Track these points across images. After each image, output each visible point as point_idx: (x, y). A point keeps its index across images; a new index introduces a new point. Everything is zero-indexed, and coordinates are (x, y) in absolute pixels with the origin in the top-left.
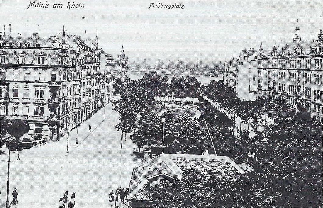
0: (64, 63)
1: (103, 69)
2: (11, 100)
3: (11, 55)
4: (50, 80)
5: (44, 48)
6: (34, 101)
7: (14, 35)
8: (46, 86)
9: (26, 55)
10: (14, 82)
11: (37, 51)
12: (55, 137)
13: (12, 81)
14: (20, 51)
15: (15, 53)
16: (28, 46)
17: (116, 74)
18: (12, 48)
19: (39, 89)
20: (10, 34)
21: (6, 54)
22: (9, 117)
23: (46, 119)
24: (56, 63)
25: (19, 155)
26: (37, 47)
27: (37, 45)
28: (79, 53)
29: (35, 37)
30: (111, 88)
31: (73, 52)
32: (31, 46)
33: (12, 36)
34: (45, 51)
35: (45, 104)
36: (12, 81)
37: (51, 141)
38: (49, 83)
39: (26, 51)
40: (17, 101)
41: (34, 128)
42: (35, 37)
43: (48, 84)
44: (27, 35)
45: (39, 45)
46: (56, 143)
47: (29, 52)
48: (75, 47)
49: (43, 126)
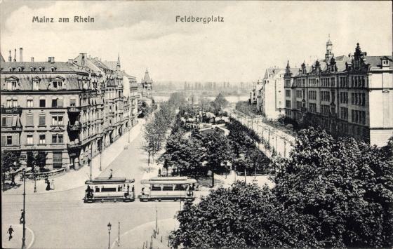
0: (350, 78)
1: (126, 93)
2: (24, 129)
3: (24, 81)
4: (69, 106)
5: (62, 72)
6: (51, 129)
7: (27, 59)
8: (64, 112)
9: (40, 80)
10: (27, 109)
11: (53, 75)
12: (76, 165)
13: (24, 109)
14: (34, 75)
15: (28, 78)
16: (43, 71)
17: (141, 97)
18: (56, 73)
19: (58, 115)
20: (21, 58)
21: (18, 80)
22: (23, 148)
23: (65, 147)
24: (74, 88)
25: (137, 201)
26: (54, 71)
27: (53, 69)
28: (101, 76)
29: (51, 60)
30: (135, 111)
31: (94, 75)
32: (45, 70)
33: (24, 60)
34: (63, 76)
35: (64, 131)
36: (24, 109)
37: (73, 170)
38: (68, 108)
39: (40, 76)
40: (43, 129)
41: (52, 157)
42: (51, 60)
43: (66, 111)
44: (41, 58)
45: (56, 69)
46: (80, 170)
47: (44, 77)
48: (97, 70)
49: (63, 154)
